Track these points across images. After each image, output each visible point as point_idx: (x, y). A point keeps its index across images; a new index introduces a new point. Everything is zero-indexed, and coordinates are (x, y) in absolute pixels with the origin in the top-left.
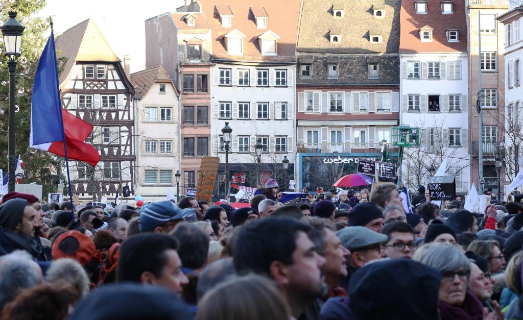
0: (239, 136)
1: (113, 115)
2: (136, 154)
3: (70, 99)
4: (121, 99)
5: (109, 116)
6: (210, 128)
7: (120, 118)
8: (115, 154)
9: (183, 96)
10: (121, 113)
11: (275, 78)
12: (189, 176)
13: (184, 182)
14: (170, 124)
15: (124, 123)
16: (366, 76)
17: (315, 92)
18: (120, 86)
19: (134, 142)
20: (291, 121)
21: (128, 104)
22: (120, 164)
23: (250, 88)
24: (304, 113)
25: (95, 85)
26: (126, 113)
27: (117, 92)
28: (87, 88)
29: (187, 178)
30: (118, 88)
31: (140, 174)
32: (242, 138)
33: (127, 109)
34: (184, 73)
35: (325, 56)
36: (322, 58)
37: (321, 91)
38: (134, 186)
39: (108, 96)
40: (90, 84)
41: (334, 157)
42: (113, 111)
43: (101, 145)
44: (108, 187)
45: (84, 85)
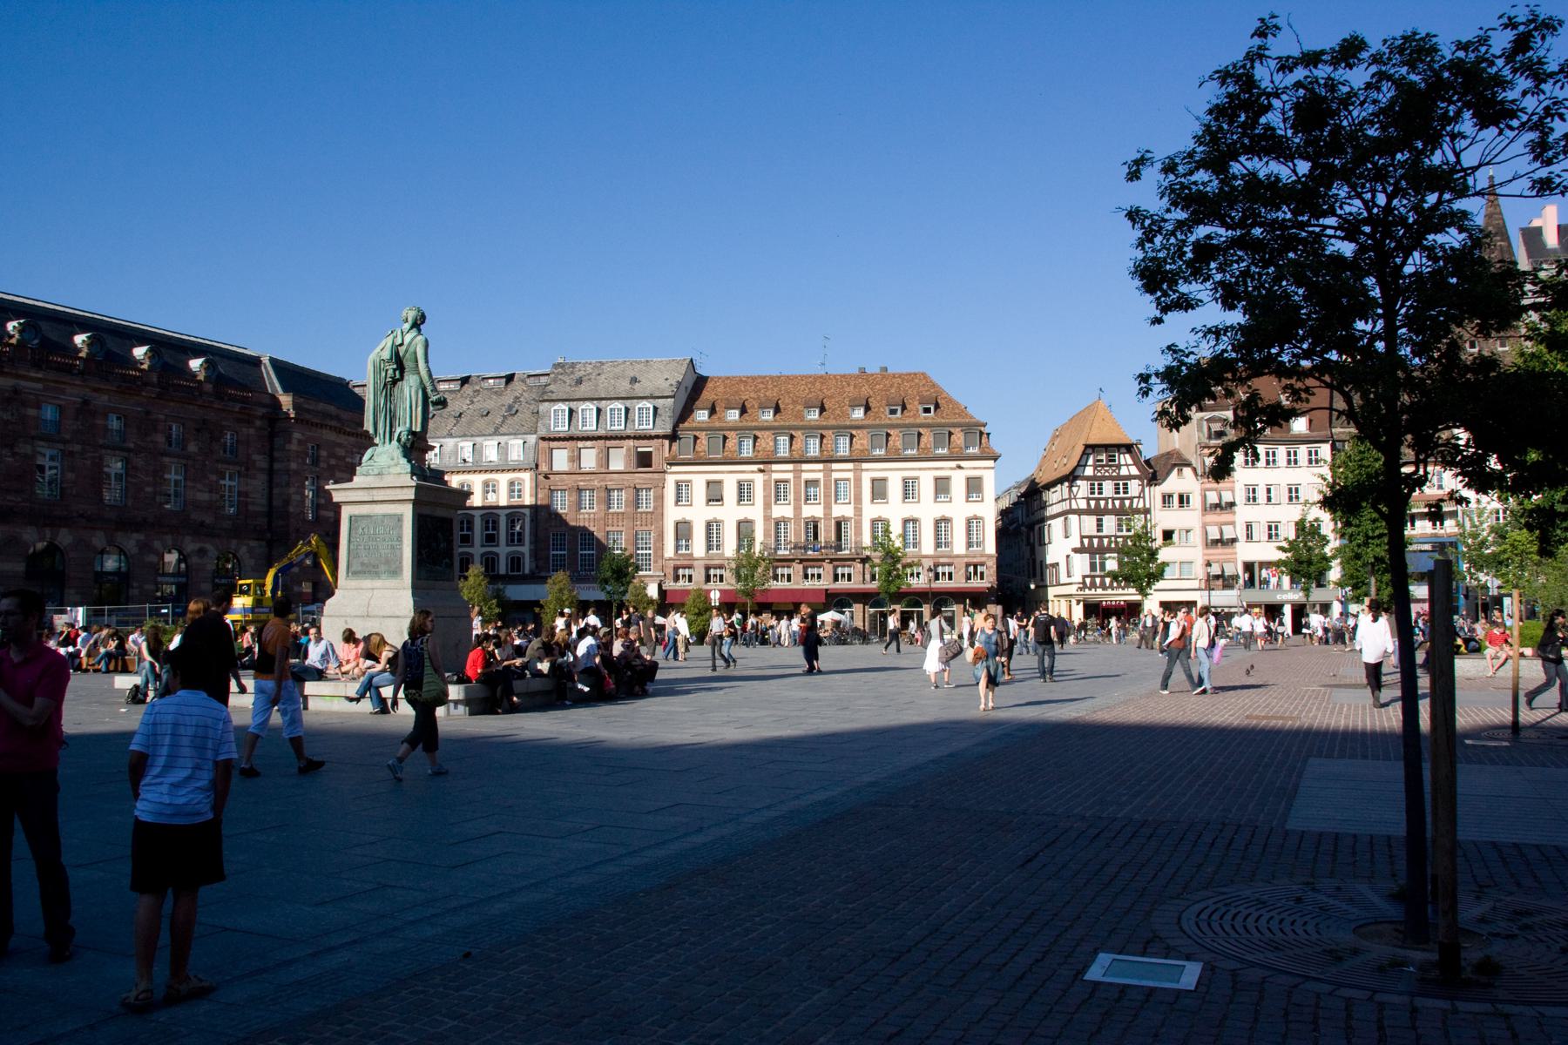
1: (1127, 503)
4: (1134, 487)
5: (1122, 504)
7: (1134, 506)
10: (1135, 500)
11: (1306, 458)
15: (1138, 511)
18: (1134, 471)
25: (1107, 471)
26: (1141, 500)
27: (1130, 477)
30: (1132, 473)
39: (1121, 483)
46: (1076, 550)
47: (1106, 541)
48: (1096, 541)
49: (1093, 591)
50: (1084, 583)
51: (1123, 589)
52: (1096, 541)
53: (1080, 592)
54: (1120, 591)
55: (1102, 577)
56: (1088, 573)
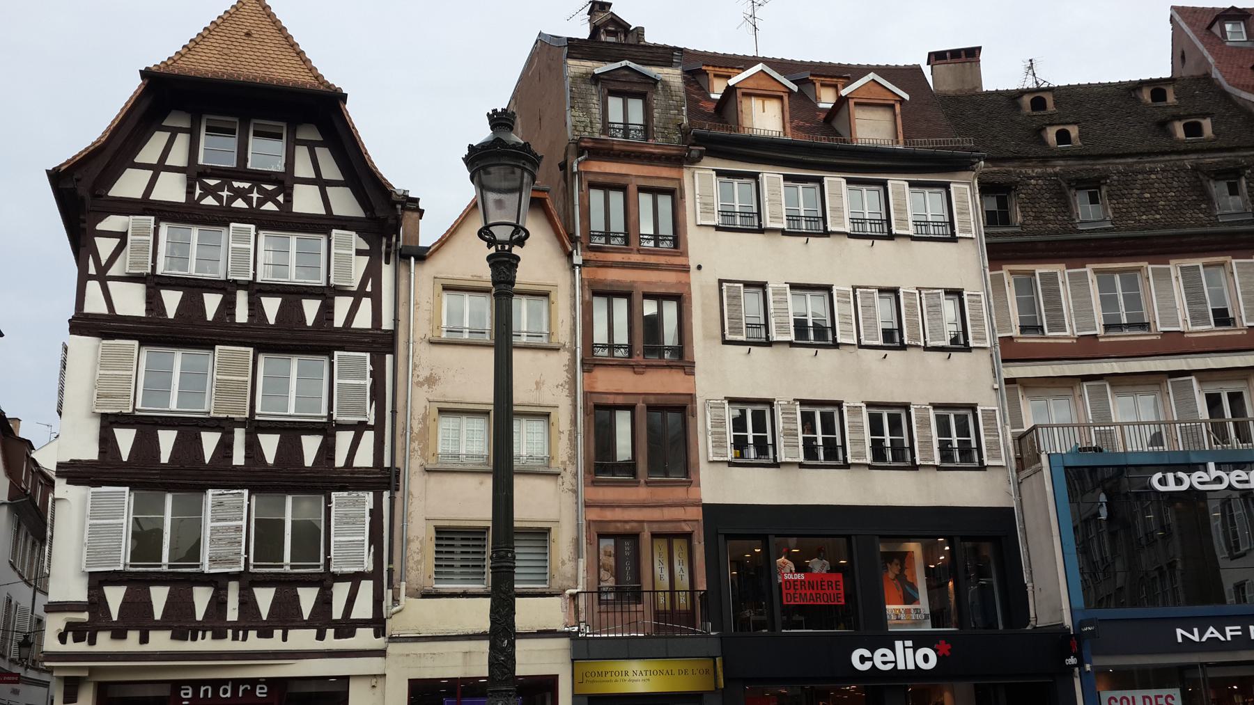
0: (803, 403)
1: (311, 308)
2: (399, 464)
3: (123, 236)
6: (693, 374)
7: (339, 321)
8: (309, 461)
9: (592, 256)
10: (342, 305)
12: (618, 555)
13: (599, 580)
14: (541, 355)
16: (1210, 215)
17: (1040, 269)
18: (344, 203)
19: (394, 412)
20: (985, 356)
21: (373, 273)
22: (328, 501)
23: (826, 240)
24: (1011, 338)
26: (366, 304)
28: (203, 202)
29: (611, 561)
30: (338, 210)
31: (415, 546)
32: (813, 413)
33: (369, 289)
34: (591, 178)
35: (1050, 170)
36: (1038, 177)
37: (1062, 266)
38: (388, 594)
40: (219, 188)
41: (1190, 468)
42: (310, 292)
43: (241, 424)
44: (265, 598)
45: (190, 191)
46: (75, 472)
47: (210, 441)
48: (167, 440)
49: (131, 643)
50: (97, 603)
51: (265, 633)
52: (167, 440)
53: (71, 646)
54: (254, 642)
55: (182, 583)
56: (122, 560)
